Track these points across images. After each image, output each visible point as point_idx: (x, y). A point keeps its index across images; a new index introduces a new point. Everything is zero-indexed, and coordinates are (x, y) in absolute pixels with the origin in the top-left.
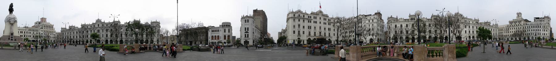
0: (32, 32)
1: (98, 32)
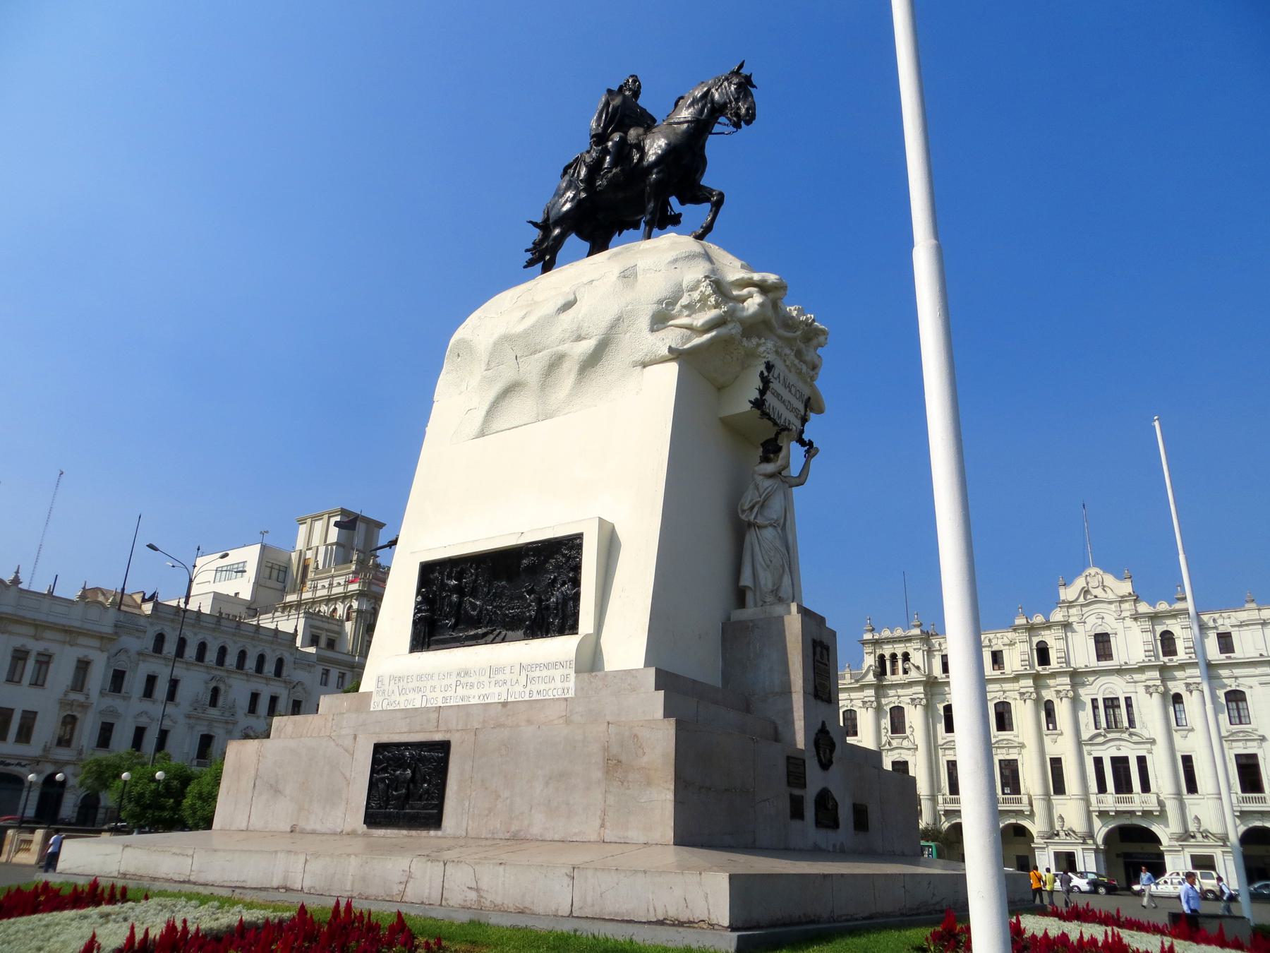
0: (194, 683)
1: (1113, 725)
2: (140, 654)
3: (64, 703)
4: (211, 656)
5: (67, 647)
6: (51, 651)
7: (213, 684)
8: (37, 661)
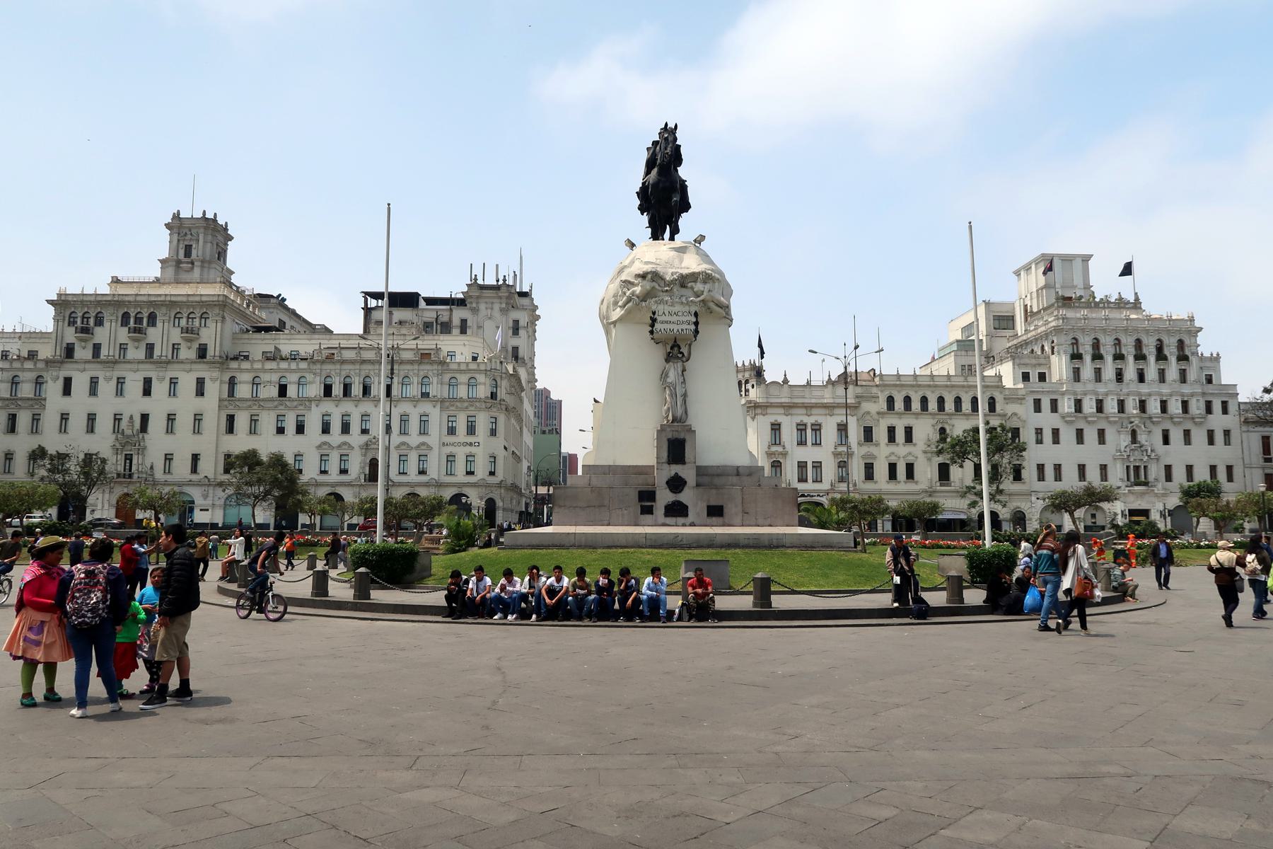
2: (878, 413)
3: (836, 455)
4: (933, 406)
5: (828, 416)
6: (819, 422)
7: (940, 426)
8: (812, 430)
